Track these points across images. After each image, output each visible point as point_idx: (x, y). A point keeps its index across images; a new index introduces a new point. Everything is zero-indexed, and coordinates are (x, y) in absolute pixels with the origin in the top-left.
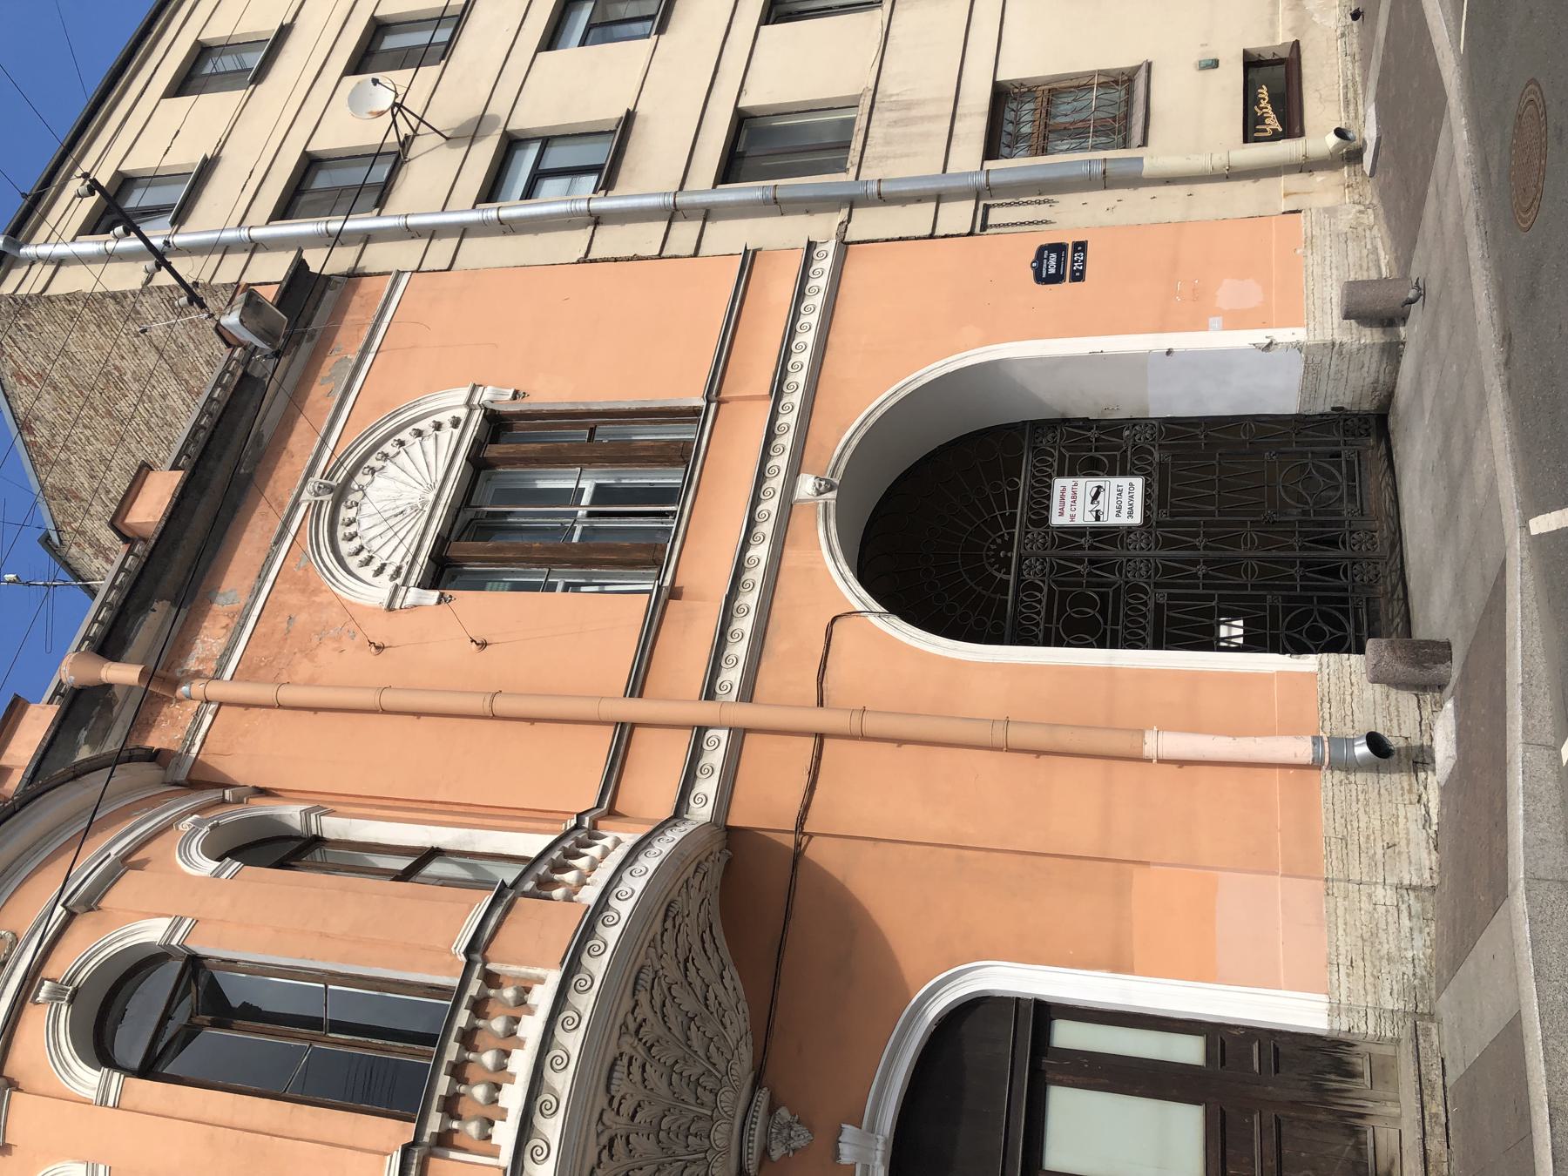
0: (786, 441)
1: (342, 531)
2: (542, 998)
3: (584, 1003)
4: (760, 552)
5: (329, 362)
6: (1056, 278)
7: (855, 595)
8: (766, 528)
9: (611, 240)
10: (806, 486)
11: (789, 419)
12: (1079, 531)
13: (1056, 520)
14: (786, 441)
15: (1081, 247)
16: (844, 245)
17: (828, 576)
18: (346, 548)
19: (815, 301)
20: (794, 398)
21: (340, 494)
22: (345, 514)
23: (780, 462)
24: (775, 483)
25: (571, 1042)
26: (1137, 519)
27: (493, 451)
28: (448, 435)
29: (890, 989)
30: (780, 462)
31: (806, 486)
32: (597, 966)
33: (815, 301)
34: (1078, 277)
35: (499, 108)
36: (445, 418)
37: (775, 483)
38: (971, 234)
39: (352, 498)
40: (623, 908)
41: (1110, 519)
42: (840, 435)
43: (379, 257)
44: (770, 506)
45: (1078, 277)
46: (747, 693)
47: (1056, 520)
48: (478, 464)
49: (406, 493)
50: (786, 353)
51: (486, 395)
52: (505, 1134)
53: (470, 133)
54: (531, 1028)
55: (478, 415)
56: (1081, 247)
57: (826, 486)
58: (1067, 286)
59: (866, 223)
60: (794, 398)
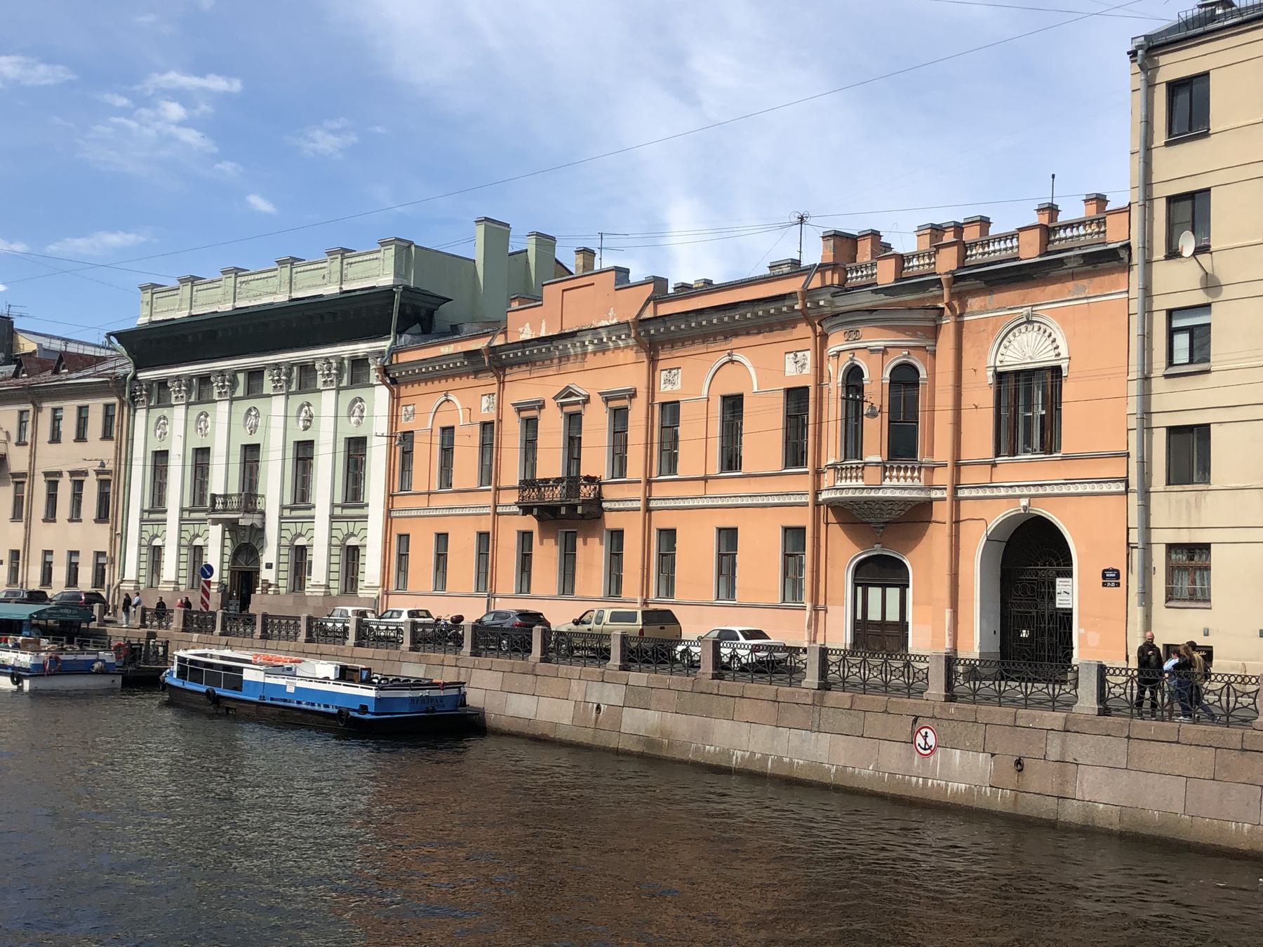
0: (1041, 491)
1: (1016, 331)
2: (860, 483)
3: (857, 494)
4: (1003, 492)
5: (1085, 282)
6: (1104, 577)
7: (992, 525)
8: (1010, 492)
10: (1024, 502)
12: (1054, 588)
13: (1058, 580)
14: (1041, 491)
15: (1118, 585)
17: (999, 515)
19: (1097, 488)
21: (1029, 322)
22: (1023, 328)
23: (1033, 491)
24: (1026, 491)
25: (850, 494)
26: (1058, 606)
29: (906, 552)
32: (865, 494)
33: (1097, 488)
34: (1104, 585)
35: (1226, 293)
37: (1026, 491)
38: (1128, 544)
39: (1030, 327)
40: (880, 494)
41: (1058, 597)
44: (1018, 492)
45: (1104, 585)
47: (1058, 580)
49: (1026, 350)
51: (1064, 365)
52: (838, 484)
54: (854, 483)
56: (1118, 585)
57: (1025, 508)
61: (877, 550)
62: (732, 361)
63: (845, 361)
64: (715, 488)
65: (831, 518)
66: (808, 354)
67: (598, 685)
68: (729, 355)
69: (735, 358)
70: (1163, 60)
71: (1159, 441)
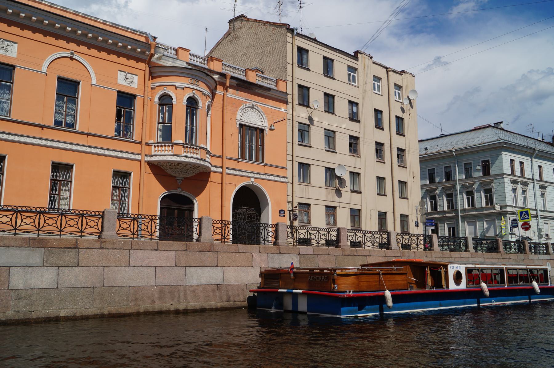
6: (280, 213)
9: (290, 146)
11: (262, 176)
14: (259, 176)
15: (284, 216)
16: (287, 183)
18: (244, 110)
20: (265, 177)
21: (252, 108)
22: (249, 109)
23: (256, 176)
27: (258, 131)
28: (260, 124)
30: (256, 176)
31: (253, 180)
34: (280, 216)
36: (263, 123)
37: (253, 175)
42: (259, 184)
43: (290, 105)
46: (227, 174)
48: (256, 129)
49: (253, 119)
50: (271, 175)
52: (185, 154)
53: (311, 119)
55: (264, 128)
58: (279, 214)
59: (290, 185)
60: (265, 177)
61: (179, 191)
62: (71, 58)
63: (189, 94)
64: (47, 133)
65: (149, 170)
66: (136, 78)
67: (277, 256)
68: (72, 54)
69: (75, 57)
70: (296, 38)
71: (296, 166)
